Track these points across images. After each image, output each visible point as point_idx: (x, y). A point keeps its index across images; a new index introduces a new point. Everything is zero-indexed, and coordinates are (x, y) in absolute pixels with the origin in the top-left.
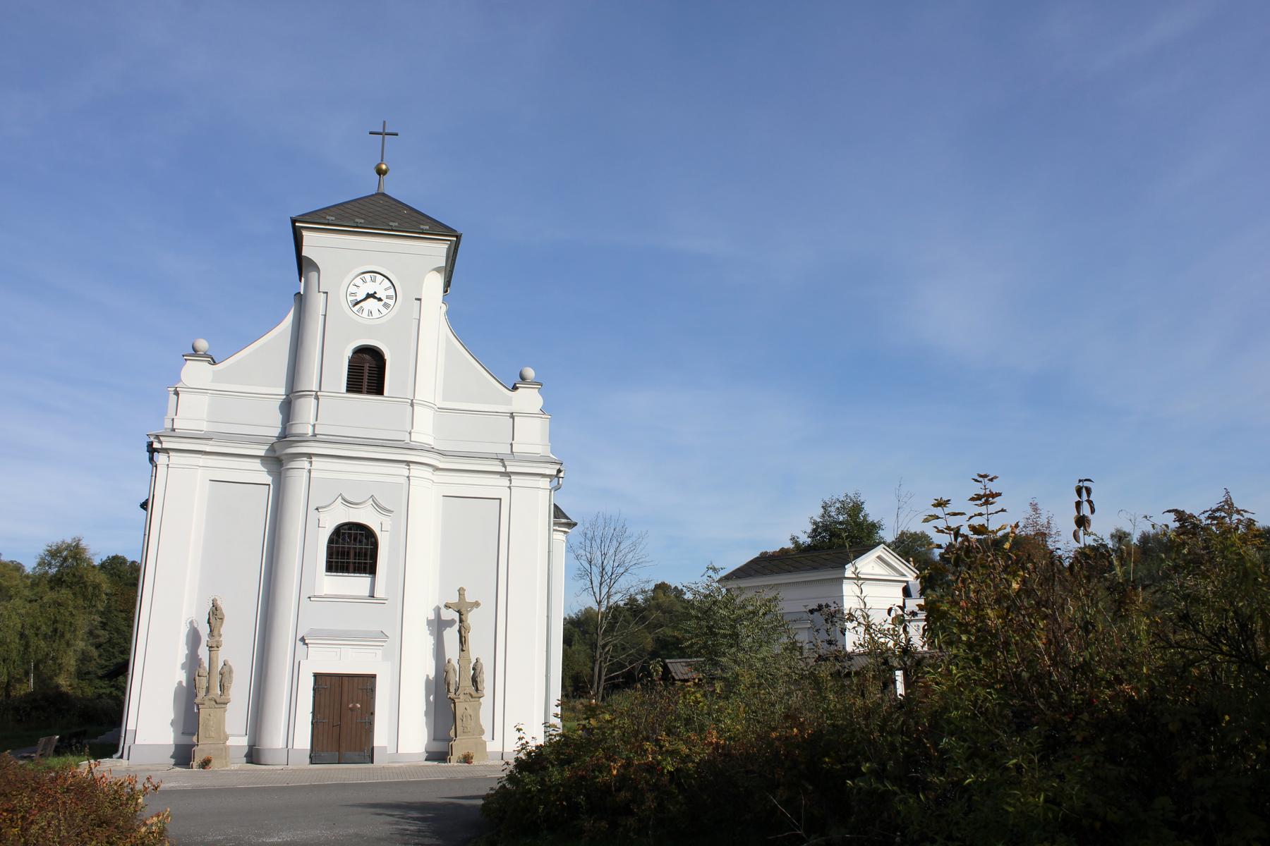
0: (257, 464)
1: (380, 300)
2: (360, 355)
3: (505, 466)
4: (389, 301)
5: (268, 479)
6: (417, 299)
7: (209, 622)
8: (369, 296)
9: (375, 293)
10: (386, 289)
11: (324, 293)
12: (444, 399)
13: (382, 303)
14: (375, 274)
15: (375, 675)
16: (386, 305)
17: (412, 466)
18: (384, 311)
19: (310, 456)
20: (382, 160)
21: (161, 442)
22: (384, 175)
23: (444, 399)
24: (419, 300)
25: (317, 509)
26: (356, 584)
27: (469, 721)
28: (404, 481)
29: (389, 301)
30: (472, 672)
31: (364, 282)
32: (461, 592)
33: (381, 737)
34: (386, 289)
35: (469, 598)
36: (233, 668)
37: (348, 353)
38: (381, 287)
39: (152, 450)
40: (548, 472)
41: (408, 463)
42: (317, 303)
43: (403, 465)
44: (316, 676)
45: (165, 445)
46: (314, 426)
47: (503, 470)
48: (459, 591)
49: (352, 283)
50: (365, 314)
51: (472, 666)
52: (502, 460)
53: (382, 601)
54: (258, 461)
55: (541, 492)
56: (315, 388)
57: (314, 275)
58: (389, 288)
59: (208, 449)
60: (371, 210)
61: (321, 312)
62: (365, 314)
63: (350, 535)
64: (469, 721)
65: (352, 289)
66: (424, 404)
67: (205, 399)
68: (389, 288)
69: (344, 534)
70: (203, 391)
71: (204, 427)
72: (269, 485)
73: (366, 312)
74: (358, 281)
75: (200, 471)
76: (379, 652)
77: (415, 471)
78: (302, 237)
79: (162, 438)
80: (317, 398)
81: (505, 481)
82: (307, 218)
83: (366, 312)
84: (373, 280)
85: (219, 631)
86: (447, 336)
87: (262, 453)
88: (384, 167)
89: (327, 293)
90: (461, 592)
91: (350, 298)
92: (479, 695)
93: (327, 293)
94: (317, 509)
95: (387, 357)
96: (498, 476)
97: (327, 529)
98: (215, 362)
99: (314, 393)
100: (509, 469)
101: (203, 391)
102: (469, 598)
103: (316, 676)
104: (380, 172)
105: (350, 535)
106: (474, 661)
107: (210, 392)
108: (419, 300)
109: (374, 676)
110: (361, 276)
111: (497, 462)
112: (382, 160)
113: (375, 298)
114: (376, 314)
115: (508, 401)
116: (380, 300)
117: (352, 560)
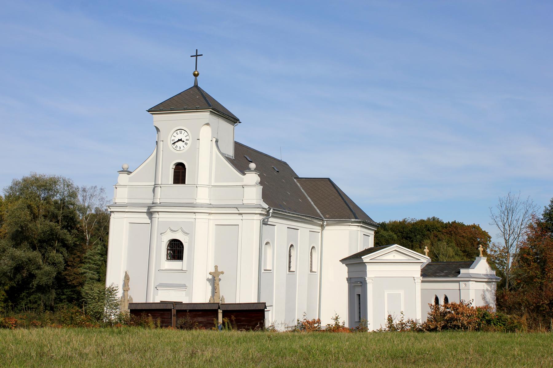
0: (145, 215)
1: (183, 141)
2: (178, 166)
3: (239, 211)
4: (187, 142)
5: (149, 221)
8: (180, 140)
9: (181, 139)
10: (186, 137)
12: (215, 182)
13: (184, 143)
16: (186, 144)
17: (197, 214)
18: (185, 146)
19: (158, 212)
20: (196, 69)
21: (110, 209)
22: (197, 76)
23: (215, 182)
24: (199, 139)
25: (161, 234)
26: (176, 264)
29: (187, 142)
31: (177, 134)
34: (186, 137)
35: (220, 270)
36: (133, 299)
38: (182, 136)
40: (257, 212)
41: (195, 213)
42: (161, 144)
43: (193, 214)
45: (112, 210)
47: (238, 212)
49: (173, 135)
52: (237, 208)
54: (145, 214)
55: (255, 221)
56: (160, 183)
57: (159, 132)
58: (187, 136)
59: (127, 210)
61: (161, 150)
63: (175, 244)
66: (203, 186)
67: (126, 190)
68: (187, 136)
69: (172, 244)
70: (125, 186)
71: (126, 201)
72: (149, 224)
73: (178, 148)
74: (175, 134)
75: (125, 219)
76: (184, 293)
77: (198, 216)
79: (110, 207)
80: (161, 187)
81: (240, 217)
82: (153, 109)
83: (178, 148)
84: (181, 133)
85: (128, 284)
86: (216, 152)
87: (146, 211)
88: (196, 73)
90: (216, 267)
94: (161, 234)
96: (238, 215)
99: (159, 185)
100: (240, 212)
101: (125, 186)
104: (196, 75)
105: (175, 244)
107: (127, 186)
108: (199, 139)
110: (176, 132)
111: (235, 209)
112: (196, 69)
113: (182, 141)
114: (182, 148)
115: (242, 180)
116: (183, 141)
117: (179, 255)
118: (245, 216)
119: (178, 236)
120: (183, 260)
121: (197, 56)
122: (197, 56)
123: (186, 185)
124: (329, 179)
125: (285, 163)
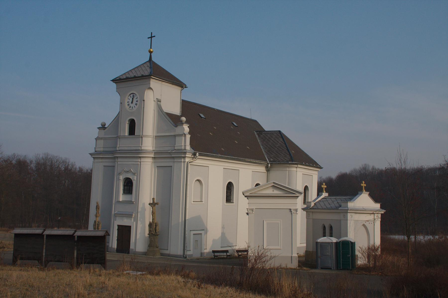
15: (131, 226)
20: (151, 48)
26: (127, 197)
33: (132, 247)
35: (155, 202)
44: (119, 226)
47: (170, 156)
50: (131, 109)
62: (131, 109)
65: (128, 100)
73: (131, 107)
81: (172, 160)
95: (136, 122)
100: (173, 156)
102: (155, 202)
109: (131, 226)
112: (151, 48)
118: (175, 160)
119: (129, 176)
120: (132, 193)
121: (151, 37)
122: (151, 37)
123: (135, 136)
124: (280, 131)
125: (256, 120)
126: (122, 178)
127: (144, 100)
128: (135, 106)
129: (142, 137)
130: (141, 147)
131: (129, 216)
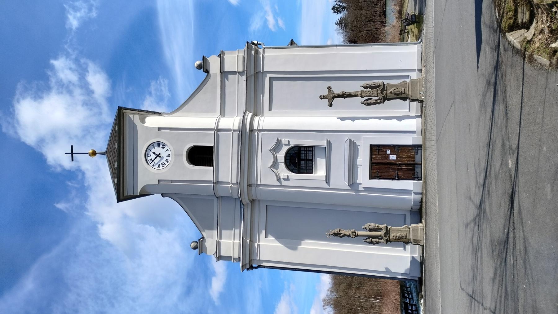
6: (159, 130)
7: (342, 237)
11: (159, 182)
14: (147, 154)
15: (370, 145)
20: (87, 153)
27: (397, 90)
28: (260, 134)
30: (369, 89)
32: (322, 97)
35: (325, 93)
37: (192, 167)
39: (251, 268)
44: (372, 177)
46: (233, 184)
47: (253, 77)
48: (321, 99)
49: (152, 166)
51: (365, 90)
53: (329, 143)
60: (113, 158)
64: (397, 90)
73: (168, 158)
78: (128, 196)
83: (168, 158)
89: (159, 181)
90: (322, 97)
91: (161, 167)
92: (382, 85)
93: (159, 181)
95: (192, 145)
97: (288, 174)
98: (202, 238)
102: (325, 93)
103: (372, 177)
106: (362, 89)
109: (370, 145)
112: (87, 153)
120: (312, 147)
126: (284, 172)
127: (159, 129)
128: (166, 148)
129: (219, 130)
130: (234, 131)
131: (353, 148)
